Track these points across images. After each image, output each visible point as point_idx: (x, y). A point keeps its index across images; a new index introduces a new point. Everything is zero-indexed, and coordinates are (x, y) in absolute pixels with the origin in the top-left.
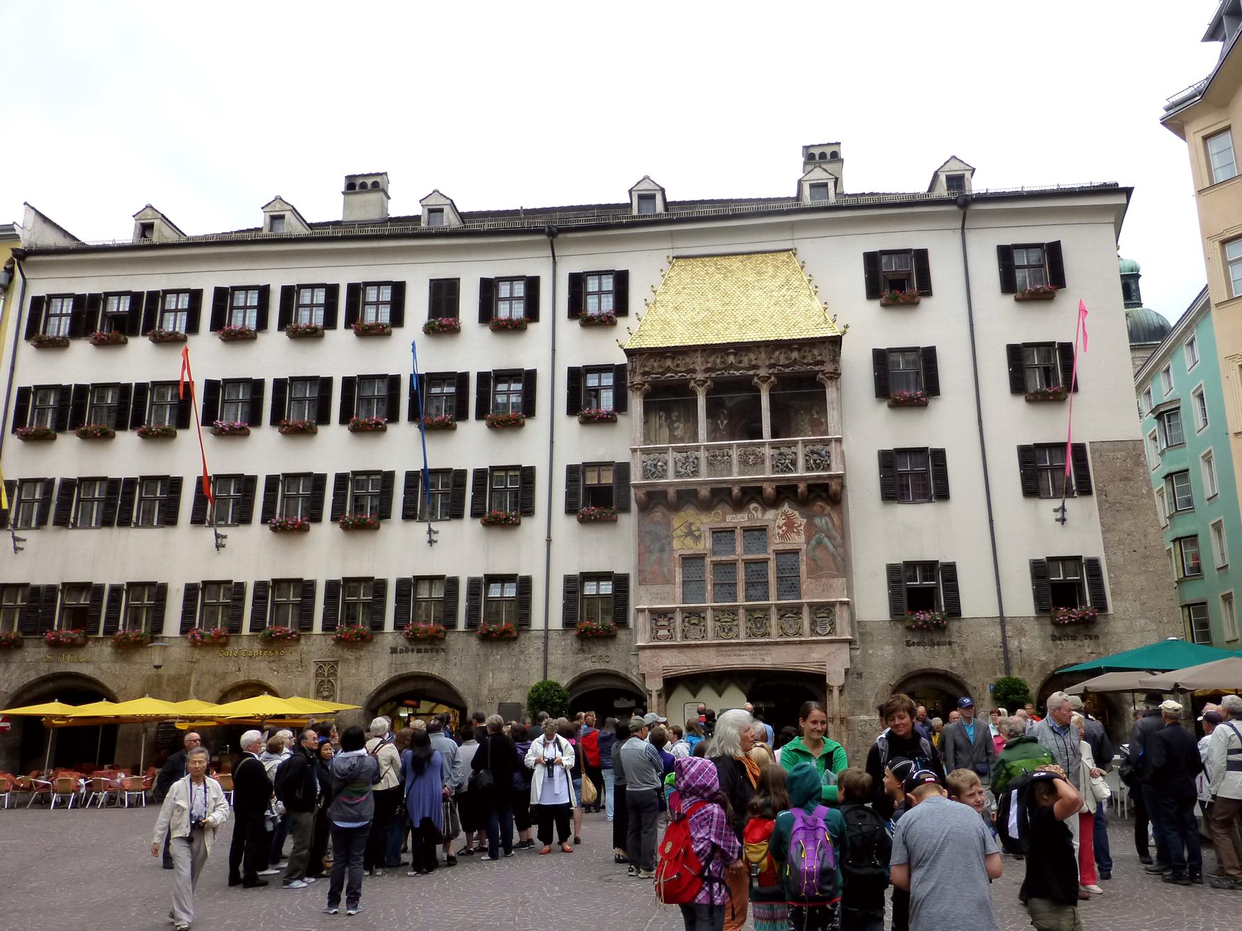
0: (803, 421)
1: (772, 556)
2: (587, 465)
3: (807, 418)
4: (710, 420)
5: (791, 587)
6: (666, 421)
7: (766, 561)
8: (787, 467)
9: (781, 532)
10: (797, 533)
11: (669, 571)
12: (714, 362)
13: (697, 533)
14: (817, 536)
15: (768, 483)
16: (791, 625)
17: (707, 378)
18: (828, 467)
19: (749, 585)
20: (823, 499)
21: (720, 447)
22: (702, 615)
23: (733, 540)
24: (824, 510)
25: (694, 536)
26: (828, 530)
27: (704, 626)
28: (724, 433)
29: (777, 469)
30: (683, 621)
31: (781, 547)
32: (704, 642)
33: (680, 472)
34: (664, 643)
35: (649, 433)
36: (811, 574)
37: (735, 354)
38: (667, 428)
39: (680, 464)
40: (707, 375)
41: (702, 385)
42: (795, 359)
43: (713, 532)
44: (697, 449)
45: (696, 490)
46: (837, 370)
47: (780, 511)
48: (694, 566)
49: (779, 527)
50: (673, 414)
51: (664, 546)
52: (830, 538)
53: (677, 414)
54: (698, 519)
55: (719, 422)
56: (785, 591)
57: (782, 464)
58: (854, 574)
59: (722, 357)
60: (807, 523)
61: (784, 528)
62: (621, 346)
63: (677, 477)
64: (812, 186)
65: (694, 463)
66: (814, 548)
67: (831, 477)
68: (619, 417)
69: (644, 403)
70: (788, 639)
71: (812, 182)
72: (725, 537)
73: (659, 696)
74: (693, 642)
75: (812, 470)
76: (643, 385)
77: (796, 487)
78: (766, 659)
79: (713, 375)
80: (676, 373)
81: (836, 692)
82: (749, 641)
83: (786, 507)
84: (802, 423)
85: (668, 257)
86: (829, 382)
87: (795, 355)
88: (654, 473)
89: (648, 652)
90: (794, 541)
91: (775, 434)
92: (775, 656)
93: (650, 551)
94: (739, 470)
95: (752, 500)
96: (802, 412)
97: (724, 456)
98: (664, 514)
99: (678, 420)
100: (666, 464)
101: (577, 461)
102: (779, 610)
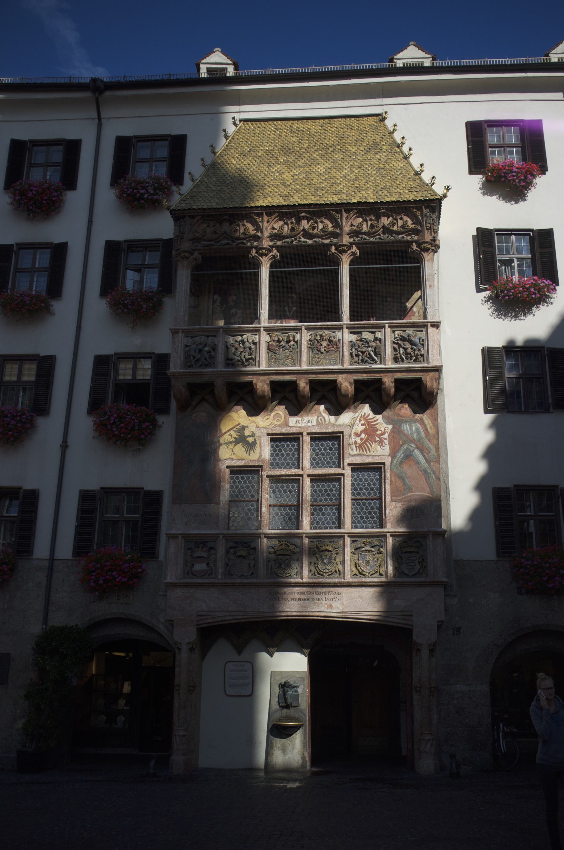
1: (348, 471)
5: (370, 513)
7: (338, 478)
9: (359, 441)
10: (380, 442)
12: (282, 227)
13: (250, 440)
14: (406, 446)
15: (344, 376)
16: (368, 562)
19: (316, 506)
21: (284, 330)
22: (253, 545)
23: (299, 450)
25: (248, 443)
26: (420, 439)
27: (254, 559)
30: (228, 552)
31: (358, 460)
32: (254, 580)
33: (232, 360)
34: (200, 581)
36: (398, 496)
40: (271, 243)
41: (266, 255)
43: (272, 440)
48: (245, 482)
49: (358, 435)
52: (422, 451)
53: (235, 298)
54: (254, 422)
55: (286, 308)
56: (362, 518)
57: (363, 353)
58: (451, 500)
60: (392, 431)
61: (363, 436)
63: (228, 365)
66: (401, 463)
69: (192, 276)
70: (364, 580)
73: (192, 650)
74: (239, 581)
76: (192, 254)
78: (333, 605)
79: (279, 243)
81: (425, 653)
82: (311, 580)
86: (425, 254)
88: (198, 360)
89: (179, 592)
90: (375, 453)
91: (353, 317)
92: (344, 603)
94: (309, 357)
96: (389, 299)
97: (288, 341)
100: (214, 348)
101: (108, 350)
102: (353, 541)
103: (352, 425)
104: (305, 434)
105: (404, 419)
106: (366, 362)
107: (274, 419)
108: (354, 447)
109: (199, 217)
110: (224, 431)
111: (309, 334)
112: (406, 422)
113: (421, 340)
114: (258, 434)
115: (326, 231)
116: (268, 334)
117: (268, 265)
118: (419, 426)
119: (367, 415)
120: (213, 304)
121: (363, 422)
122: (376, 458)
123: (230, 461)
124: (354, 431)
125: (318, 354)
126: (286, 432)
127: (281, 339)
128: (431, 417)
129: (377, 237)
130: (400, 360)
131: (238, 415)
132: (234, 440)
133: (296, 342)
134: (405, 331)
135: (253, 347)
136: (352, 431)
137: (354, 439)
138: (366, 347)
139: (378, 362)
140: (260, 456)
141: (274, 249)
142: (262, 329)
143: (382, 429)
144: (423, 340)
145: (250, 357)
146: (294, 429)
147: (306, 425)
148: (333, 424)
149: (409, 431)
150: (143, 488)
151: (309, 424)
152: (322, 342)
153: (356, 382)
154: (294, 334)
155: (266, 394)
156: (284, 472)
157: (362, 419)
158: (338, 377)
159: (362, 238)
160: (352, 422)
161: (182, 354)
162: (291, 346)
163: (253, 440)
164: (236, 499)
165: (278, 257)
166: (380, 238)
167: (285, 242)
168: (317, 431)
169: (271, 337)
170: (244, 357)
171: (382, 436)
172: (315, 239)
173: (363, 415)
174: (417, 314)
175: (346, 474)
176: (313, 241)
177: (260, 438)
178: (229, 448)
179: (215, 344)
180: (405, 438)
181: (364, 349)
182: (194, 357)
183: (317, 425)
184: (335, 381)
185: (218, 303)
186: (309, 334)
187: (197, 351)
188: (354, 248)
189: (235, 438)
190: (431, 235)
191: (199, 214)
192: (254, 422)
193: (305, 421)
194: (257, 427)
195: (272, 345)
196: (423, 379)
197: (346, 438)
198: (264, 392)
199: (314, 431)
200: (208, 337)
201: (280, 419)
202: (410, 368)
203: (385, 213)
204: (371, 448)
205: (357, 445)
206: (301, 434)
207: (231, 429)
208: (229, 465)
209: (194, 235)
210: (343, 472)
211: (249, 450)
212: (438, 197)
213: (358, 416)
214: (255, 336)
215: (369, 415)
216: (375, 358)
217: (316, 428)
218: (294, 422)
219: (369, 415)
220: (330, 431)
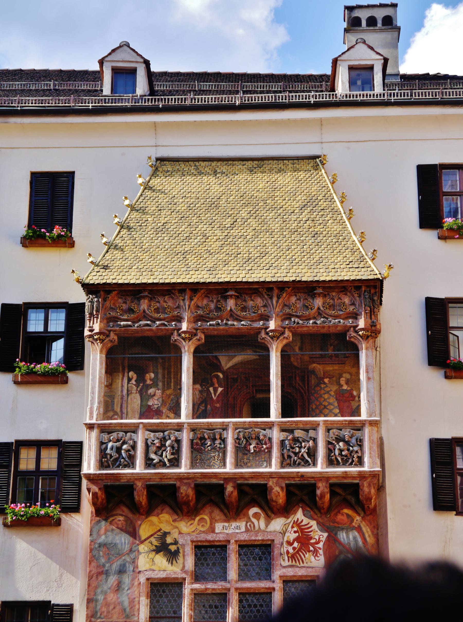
0: (328, 392)
1: (278, 585)
2: (21, 444)
3: (335, 388)
4: (198, 386)
6: (137, 385)
8: (303, 458)
9: (291, 551)
11: (132, 602)
13: (173, 548)
15: (275, 480)
17: (196, 329)
18: (360, 462)
20: (351, 507)
21: (211, 428)
23: (225, 559)
24: (352, 521)
25: (170, 551)
28: (218, 405)
29: (288, 461)
31: (290, 572)
35: (113, 402)
37: (237, 298)
38: (138, 396)
39: (153, 449)
41: (190, 339)
42: (319, 308)
43: (196, 547)
44: (179, 428)
45: (174, 485)
46: (375, 326)
47: (290, 520)
48: (167, 596)
50: (147, 375)
51: (124, 565)
53: (152, 375)
54: (177, 528)
55: (211, 389)
57: (296, 454)
59: (218, 301)
61: (296, 544)
62: (78, 281)
64: (351, 68)
65: (173, 447)
67: (362, 476)
68: (70, 375)
71: (352, 63)
72: (214, 554)
75: (338, 464)
76: (108, 336)
77: (314, 487)
80: (154, 320)
83: (299, 515)
84: (326, 396)
85: (150, 158)
87: (319, 302)
88: (116, 460)
90: (309, 564)
93: (107, 573)
95: (253, 503)
96: (326, 380)
98: (127, 519)
99: (155, 384)
100: (134, 447)
103: (284, 531)
104: (232, 541)
105: (340, 526)
106: (299, 465)
107: (198, 525)
108: (286, 558)
109: (116, 292)
110: (143, 538)
111: (238, 431)
112: (343, 529)
113: (358, 441)
114: (181, 541)
115: (256, 313)
116: (193, 430)
117: (192, 350)
118: (357, 534)
119: (300, 521)
120: (128, 383)
121: (295, 529)
122: (310, 570)
123: (151, 572)
124: (286, 539)
125: (247, 454)
126: (212, 539)
127: (206, 437)
128: (369, 524)
129: (311, 322)
130: (335, 462)
131: (160, 519)
132: (154, 548)
133: (224, 440)
134: (341, 430)
135: (176, 445)
136: (283, 539)
137: (286, 548)
138: (298, 447)
139: (312, 464)
140: (184, 567)
141: (198, 331)
142: (186, 426)
143: (317, 537)
144: (361, 441)
145: (172, 456)
146: (221, 535)
147: (234, 531)
148: (264, 531)
149: (346, 539)
150: (50, 602)
151: (237, 531)
152: (251, 441)
153: (288, 486)
154: (222, 430)
155: (190, 499)
156: (210, 586)
157: (294, 525)
158: (269, 481)
159: (294, 322)
160: (284, 529)
161: (98, 452)
162: (218, 446)
163: (176, 549)
164: (157, 615)
165: (203, 341)
166: (315, 323)
167: (210, 325)
168: (247, 539)
169: (195, 433)
170: (166, 457)
171: (316, 545)
172: (242, 323)
173: (296, 520)
174: (357, 398)
175: (277, 588)
176: (242, 325)
177: (183, 547)
178: (150, 557)
179: (134, 442)
180: (341, 547)
181: (297, 450)
182: (111, 456)
183: (245, 532)
184: (265, 486)
185: (133, 382)
186: (238, 431)
187: (114, 449)
188: (287, 333)
189: (156, 546)
190: (371, 319)
191: (115, 289)
192: (177, 528)
193: (233, 527)
194: (180, 533)
195: (197, 444)
196: (360, 485)
197: (278, 547)
198: (188, 496)
199: (242, 539)
200: (126, 432)
201: (205, 525)
202: (346, 472)
203: (322, 293)
204: (304, 559)
205: (290, 555)
206: (229, 541)
207: (152, 535)
208: (149, 577)
209: (109, 313)
210: (275, 585)
211: (171, 560)
212: (379, 276)
213: (290, 522)
214: (178, 433)
215: (302, 521)
216: (309, 460)
217: (245, 536)
218: (221, 528)
219: (302, 521)
220: (260, 538)
